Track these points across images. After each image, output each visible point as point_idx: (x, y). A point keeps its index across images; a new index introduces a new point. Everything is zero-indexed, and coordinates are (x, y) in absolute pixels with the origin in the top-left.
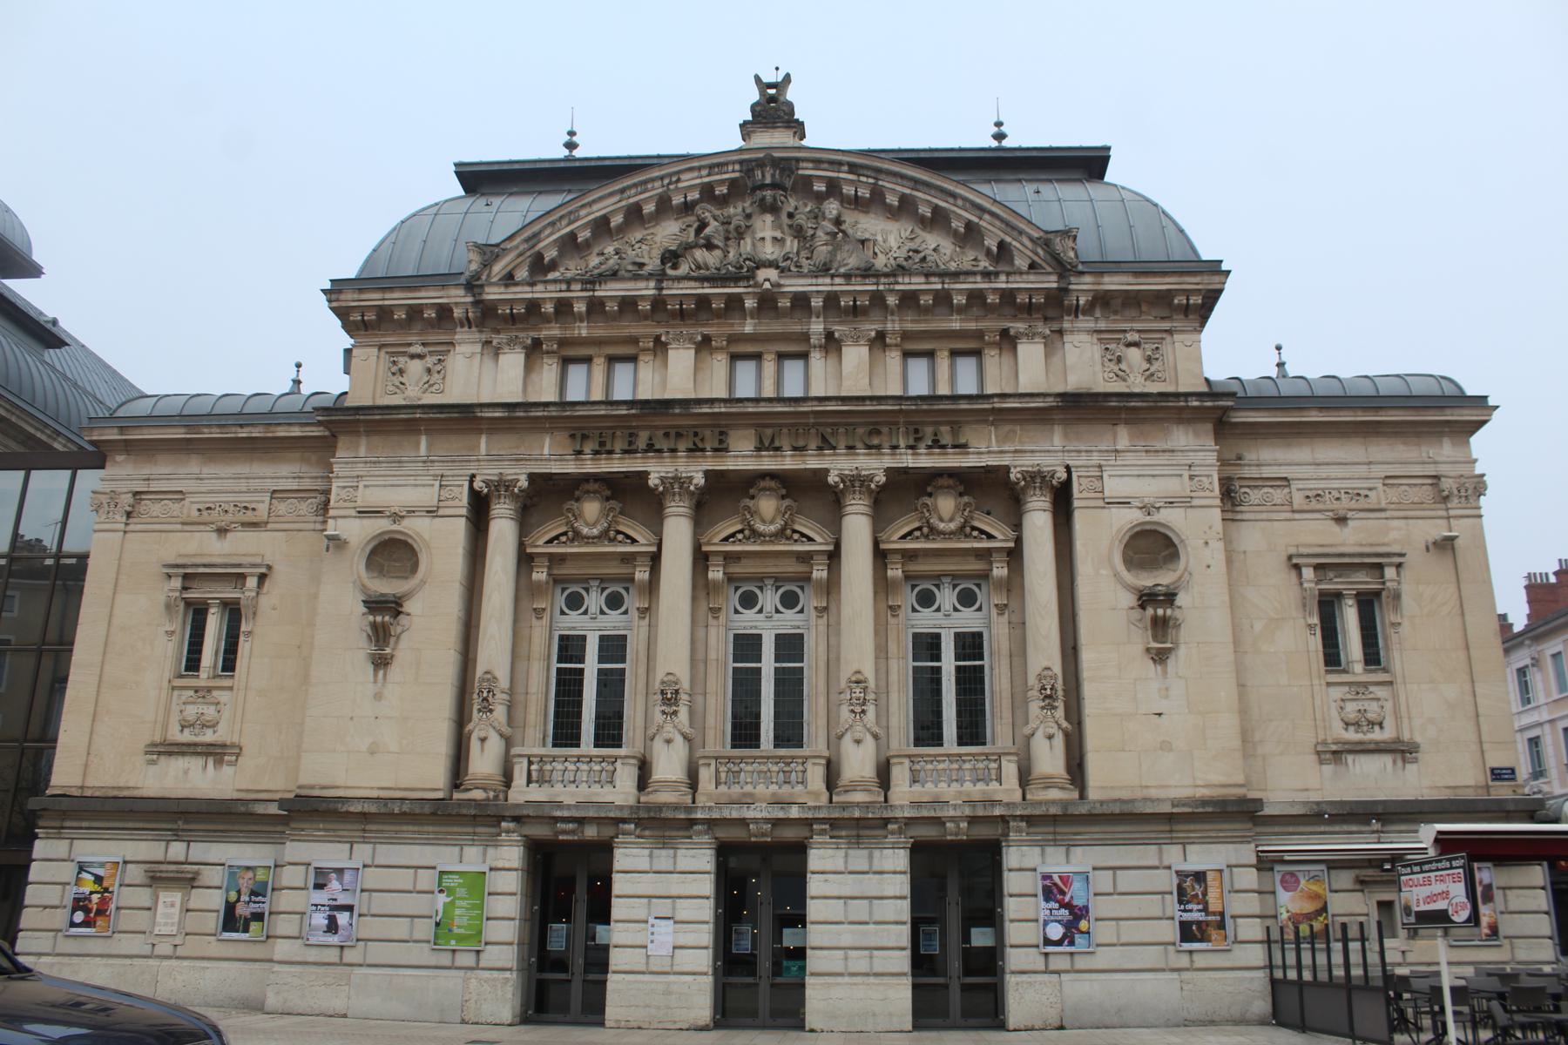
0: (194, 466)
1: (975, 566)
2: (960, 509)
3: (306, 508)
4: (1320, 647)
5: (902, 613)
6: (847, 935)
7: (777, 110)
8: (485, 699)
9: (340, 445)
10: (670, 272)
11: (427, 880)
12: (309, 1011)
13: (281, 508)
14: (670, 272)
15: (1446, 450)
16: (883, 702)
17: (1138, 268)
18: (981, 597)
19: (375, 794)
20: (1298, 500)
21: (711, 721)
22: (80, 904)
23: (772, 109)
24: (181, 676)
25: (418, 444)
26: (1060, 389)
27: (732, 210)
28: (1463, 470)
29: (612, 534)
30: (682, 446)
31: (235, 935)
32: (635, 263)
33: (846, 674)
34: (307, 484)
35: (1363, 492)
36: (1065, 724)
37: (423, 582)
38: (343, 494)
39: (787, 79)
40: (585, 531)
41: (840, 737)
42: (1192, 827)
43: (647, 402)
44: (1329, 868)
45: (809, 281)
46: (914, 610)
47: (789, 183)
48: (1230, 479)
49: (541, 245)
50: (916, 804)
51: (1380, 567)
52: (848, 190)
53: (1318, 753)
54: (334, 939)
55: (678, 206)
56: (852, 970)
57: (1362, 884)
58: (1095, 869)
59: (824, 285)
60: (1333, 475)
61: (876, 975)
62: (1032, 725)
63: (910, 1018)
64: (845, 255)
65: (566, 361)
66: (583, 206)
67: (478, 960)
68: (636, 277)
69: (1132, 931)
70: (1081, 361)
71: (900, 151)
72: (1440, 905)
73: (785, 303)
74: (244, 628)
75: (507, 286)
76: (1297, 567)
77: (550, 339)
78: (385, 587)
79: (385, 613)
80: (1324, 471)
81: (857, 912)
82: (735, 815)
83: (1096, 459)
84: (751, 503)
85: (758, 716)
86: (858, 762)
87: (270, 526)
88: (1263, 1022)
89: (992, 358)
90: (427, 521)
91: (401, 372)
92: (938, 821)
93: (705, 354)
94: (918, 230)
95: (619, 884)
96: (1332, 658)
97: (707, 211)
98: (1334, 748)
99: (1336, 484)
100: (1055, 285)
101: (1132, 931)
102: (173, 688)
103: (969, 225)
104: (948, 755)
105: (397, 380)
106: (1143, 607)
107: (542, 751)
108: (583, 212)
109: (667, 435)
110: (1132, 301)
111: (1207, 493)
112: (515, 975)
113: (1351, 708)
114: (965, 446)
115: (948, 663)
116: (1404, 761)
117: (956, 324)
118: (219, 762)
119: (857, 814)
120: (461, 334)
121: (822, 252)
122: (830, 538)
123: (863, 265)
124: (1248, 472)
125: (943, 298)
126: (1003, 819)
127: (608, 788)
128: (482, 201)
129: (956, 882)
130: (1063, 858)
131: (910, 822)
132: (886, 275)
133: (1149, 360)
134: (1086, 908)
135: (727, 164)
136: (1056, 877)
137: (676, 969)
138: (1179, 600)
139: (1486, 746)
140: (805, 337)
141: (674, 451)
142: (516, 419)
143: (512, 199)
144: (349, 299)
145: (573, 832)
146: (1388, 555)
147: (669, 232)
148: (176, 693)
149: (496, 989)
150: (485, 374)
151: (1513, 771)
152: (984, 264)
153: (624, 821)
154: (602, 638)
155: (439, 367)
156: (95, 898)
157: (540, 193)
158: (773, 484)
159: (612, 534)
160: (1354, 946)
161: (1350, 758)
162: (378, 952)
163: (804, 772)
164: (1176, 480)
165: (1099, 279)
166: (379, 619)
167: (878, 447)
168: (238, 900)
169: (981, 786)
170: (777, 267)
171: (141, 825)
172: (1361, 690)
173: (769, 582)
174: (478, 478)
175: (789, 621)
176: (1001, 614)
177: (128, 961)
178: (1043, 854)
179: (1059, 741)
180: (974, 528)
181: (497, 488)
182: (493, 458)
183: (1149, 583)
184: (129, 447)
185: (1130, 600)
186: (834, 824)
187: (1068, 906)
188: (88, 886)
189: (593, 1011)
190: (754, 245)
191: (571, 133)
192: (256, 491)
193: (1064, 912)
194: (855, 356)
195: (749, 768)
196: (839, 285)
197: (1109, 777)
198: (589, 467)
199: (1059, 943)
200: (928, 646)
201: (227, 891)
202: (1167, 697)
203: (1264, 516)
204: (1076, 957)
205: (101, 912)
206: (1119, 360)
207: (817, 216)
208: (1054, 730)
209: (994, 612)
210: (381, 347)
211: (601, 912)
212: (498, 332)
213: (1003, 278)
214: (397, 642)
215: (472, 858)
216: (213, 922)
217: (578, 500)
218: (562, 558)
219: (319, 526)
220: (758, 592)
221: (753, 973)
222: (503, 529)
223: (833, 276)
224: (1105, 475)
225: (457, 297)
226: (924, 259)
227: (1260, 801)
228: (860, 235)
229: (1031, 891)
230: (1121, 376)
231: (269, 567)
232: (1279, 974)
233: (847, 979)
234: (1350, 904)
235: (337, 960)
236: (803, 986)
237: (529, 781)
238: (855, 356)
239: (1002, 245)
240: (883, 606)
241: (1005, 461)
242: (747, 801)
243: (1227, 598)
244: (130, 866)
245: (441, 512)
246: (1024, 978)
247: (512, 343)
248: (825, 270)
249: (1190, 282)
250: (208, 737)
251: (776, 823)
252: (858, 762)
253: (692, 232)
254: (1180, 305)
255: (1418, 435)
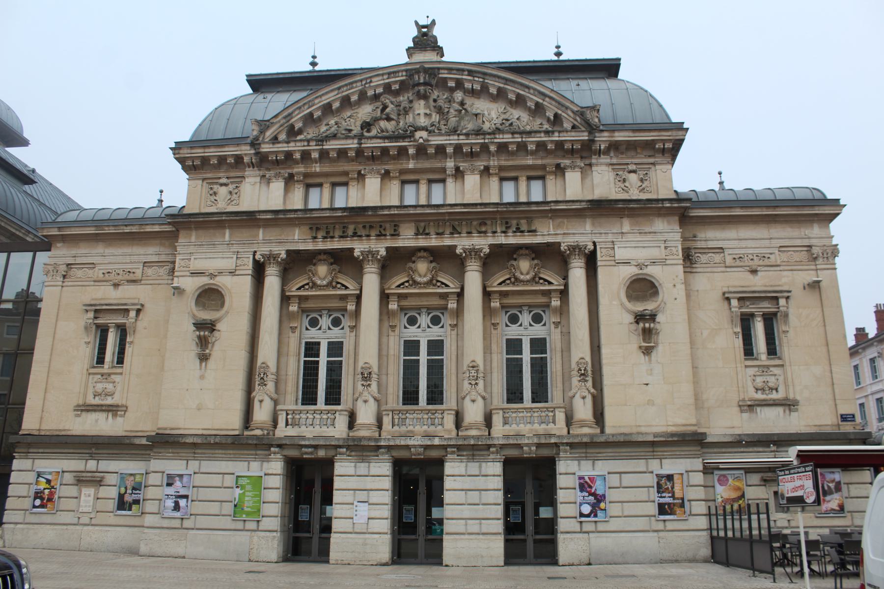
0: (100, 249)
1: (542, 300)
2: (532, 267)
3: (163, 271)
4: (742, 345)
5: (499, 327)
6: (467, 511)
7: (427, 40)
8: (262, 378)
9: (181, 235)
10: (366, 134)
11: (229, 481)
12: (164, 555)
13: (149, 271)
14: (366, 134)
15: (815, 231)
16: (488, 379)
17: (635, 127)
18: (545, 318)
19: (200, 432)
20: (729, 260)
21: (391, 390)
22: (38, 495)
23: (425, 40)
24: (94, 367)
25: (225, 234)
26: (590, 198)
27: (401, 98)
28: (825, 242)
29: (334, 284)
30: (373, 233)
31: (124, 512)
32: (346, 130)
33: (467, 362)
34: (163, 258)
35: (767, 256)
36: (592, 390)
37: (227, 312)
38: (183, 263)
39: (433, 23)
40: (319, 282)
41: (463, 398)
42: (665, 449)
43: (353, 208)
44: (746, 473)
45: (445, 138)
46: (507, 326)
47: (434, 82)
48: (689, 248)
49: (293, 120)
50: (506, 437)
51: (777, 298)
52: (468, 85)
53: (740, 406)
54: (178, 514)
55: (371, 96)
56: (469, 531)
57: (765, 482)
58: (609, 473)
59: (454, 140)
60: (749, 246)
61: (484, 534)
62: (573, 391)
63: (502, 559)
64: (466, 123)
65: (308, 186)
66: (317, 98)
67: (258, 526)
68: (347, 138)
69: (630, 509)
70: (603, 181)
71: (499, 63)
72: (799, 493)
73: (431, 151)
74: (128, 339)
75: (273, 144)
76: (728, 299)
77: (298, 173)
78: (206, 315)
79: (206, 330)
80: (744, 244)
81: (472, 498)
82: (403, 443)
83: (610, 238)
84: (412, 265)
85: (418, 387)
86: (474, 413)
87: (143, 282)
88: (706, 561)
89: (551, 180)
90: (229, 277)
91: (215, 194)
92: (519, 446)
93: (386, 181)
94: (508, 108)
95: (338, 483)
96: (749, 351)
97: (387, 99)
98: (749, 403)
99: (751, 251)
100: (586, 138)
101: (630, 509)
102: (89, 374)
103: (537, 104)
104: (525, 408)
105: (213, 198)
106: (637, 322)
107: (294, 407)
108: (316, 101)
109: (364, 227)
110: (631, 147)
111: (675, 257)
112: (279, 534)
113: (759, 380)
114: (535, 231)
115: (526, 356)
116: (790, 410)
117: (530, 161)
118: (115, 415)
119: (472, 442)
120: (249, 172)
121: (453, 121)
122: (458, 285)
123: (476, 128)
124: (700, 244)
125: (522, 147)
126: (556, 445)
127: (331, 428)
128: (261, 96)
129: (529, 481)
130: (591, 467)
131: (503, 447)
132: (489, 134)
133: (642, 180)
134: (604, 496)
135: (398, 72)
136: (587, 479)
137: (370, 531)
138: (658, 319)
139: (838, 402)
140: (444, 170)
141: (368, 236)
142: (279, 219)
143: (278, 95)
144: (185, 152)
145: (311, 453)
146: (781, 292)
147: (366, 111)
148: (91, 377)
149: (269, 542)
150: (262, 194)
151: (854, 416)
152: (546, 126)
153: (340, 447)
154: (329, 343)
155: (236, 191)
156: (47, 491)
157: (295, 91)
158: (425, 254)
159: (334, 284)
160: (763, 517)
161: (759, 409)
162: (202, 522)
163: (443, 418)
164: (657, 249)
165: (612, 134)
166: (202, 333)
167: (485, 232)
168: (126, 493)
169: (543, 426)
170: (427, 130)
171: (71, 451)
172: (765, 370)
173: (425, 310)
174: (258, 253)
175: (435, 333)
176: (556, 327)
177: (65, 527)
178: (579, 465)
179: (589, 400)
180: (541, 278)
181: (269, 258)
182: (267, 242)
183: (641, 309)
184: (64, 239)
185: (631, 318)
186: (459, 448)
187: (594, 494)
188: (43, 485)
189: (323, 555)
190: (414, 118)
191: (314, 57)
192: (135, 262)
193: (591, 498)
194: (472, 180)
195: (411, 416)
196: (462, 140)
197: (618, 421)
198: (321, 246)
199: (588, 516)
200: (514, 346)
201: (120, 487)
202: (651, 374)
203: (709, 270)
204: (599, 524)
205: (50, 500)
206: (624, 181)
207: (450, 101)
208: (586, 394)
209: (553, 326)
210: (204, 180)
211: (328, 499)
212: (269, 170)
213: (556, 134)
214: (213, 347)
215: (255, 468)
216: (112, 505)
217: (314, 265)
218: (306, 298)
219: (170, 282)
220: (418, 316)
221: (414, 533)
222: (272, 282)
223: (459, 135)
224: (616, 247)
225: (246, 150)
226: (511, 124)
227: (705, 434)
228: (474, 111)
229: (572, 486)
230: (625, 190)
231: (142, 305)
232: (715, 533)
233: (467, 536)
234: (756, 493)
235: (179, 526)
236: (442, 540)
237: (287, 424)
238: (472, 180)
239: (556, 116)
240: (489, 324)
242: (410, 435)
243: (686, 317)
244: (65, 474)
245: (237, 273)
246: (568, 535)
247: (277, 176)
248: (454, 131)
249: (665, 136)
250: (109, 401)
251: (426, 447)
252: (474, 413)
253: (379, 111)
254: (659, 149)
255: (799, 222)
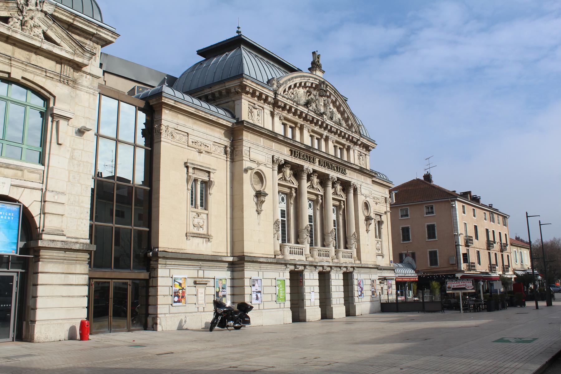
22: (176, 294)
120: (266, 106)
156: (181, 291)
188: (178, 288)
191: (238, 28)
205: (183, 297)
239: (352, 124)
241: (350, 180)
